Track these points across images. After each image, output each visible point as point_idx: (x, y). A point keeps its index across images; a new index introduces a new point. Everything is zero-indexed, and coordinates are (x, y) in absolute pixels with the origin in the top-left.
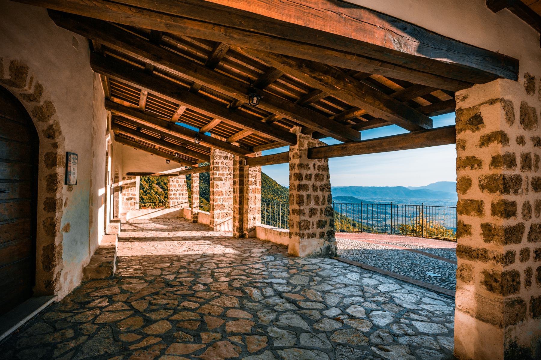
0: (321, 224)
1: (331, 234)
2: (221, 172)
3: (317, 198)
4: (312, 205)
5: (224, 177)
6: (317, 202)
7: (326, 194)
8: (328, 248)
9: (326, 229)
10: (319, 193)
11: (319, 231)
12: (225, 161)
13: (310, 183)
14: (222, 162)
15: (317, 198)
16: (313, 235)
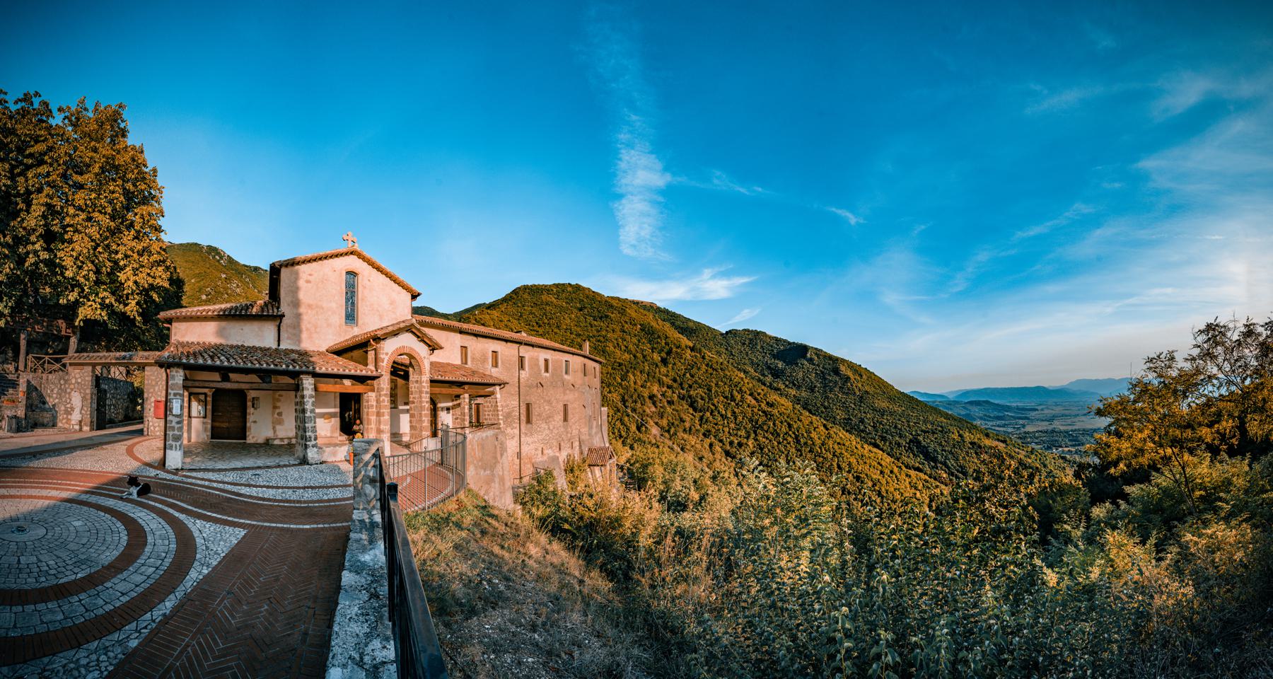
12: (417, 385)
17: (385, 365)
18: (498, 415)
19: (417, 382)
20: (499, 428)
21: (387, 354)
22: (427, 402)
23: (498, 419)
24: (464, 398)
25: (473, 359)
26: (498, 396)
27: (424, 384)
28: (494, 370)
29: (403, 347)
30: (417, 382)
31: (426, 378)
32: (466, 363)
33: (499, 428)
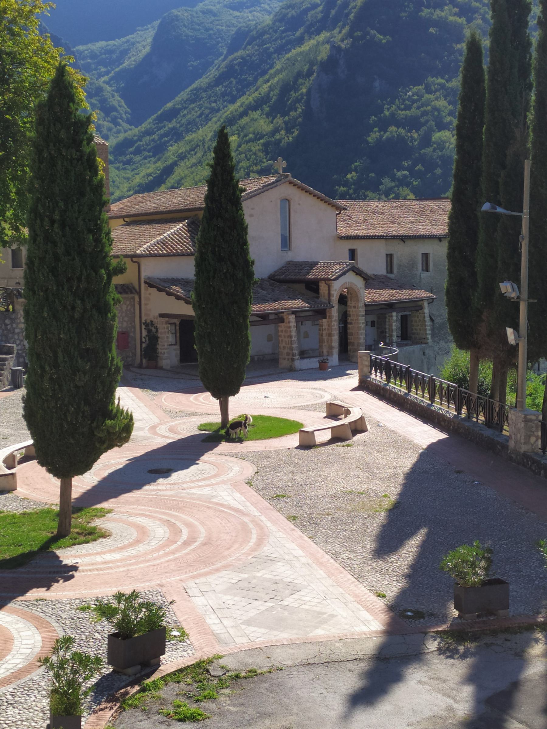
0: (288, 354)
1: (293, 360)
2: (352, 318)
3: (286, 342)
4: (284, 344)
5: (353, 322)
6: (286, 344)
7: (289, 339)
8: (291, 366)
9: (290, 357)
10: (287, 339)
11: (287, 357)
12: (354, 310)
13: (283, 334)
14: (352, 311)
15: (286, 342)
16: (285, 359)
17: (335, 299)
18: (426, 330)
19: (355, 307)
20: (426, 343)
21: (336, 290)
22: (363, 323)
23: (426, 334)
24: (392, 316)
25: (400, 266)
26: (426, 311)
27: (361, 309)
28: (425, 275)
29: (346, 283)
30: (355, 307)
31: (361, 304)
32: (391, 272)
33: (426, 343)
